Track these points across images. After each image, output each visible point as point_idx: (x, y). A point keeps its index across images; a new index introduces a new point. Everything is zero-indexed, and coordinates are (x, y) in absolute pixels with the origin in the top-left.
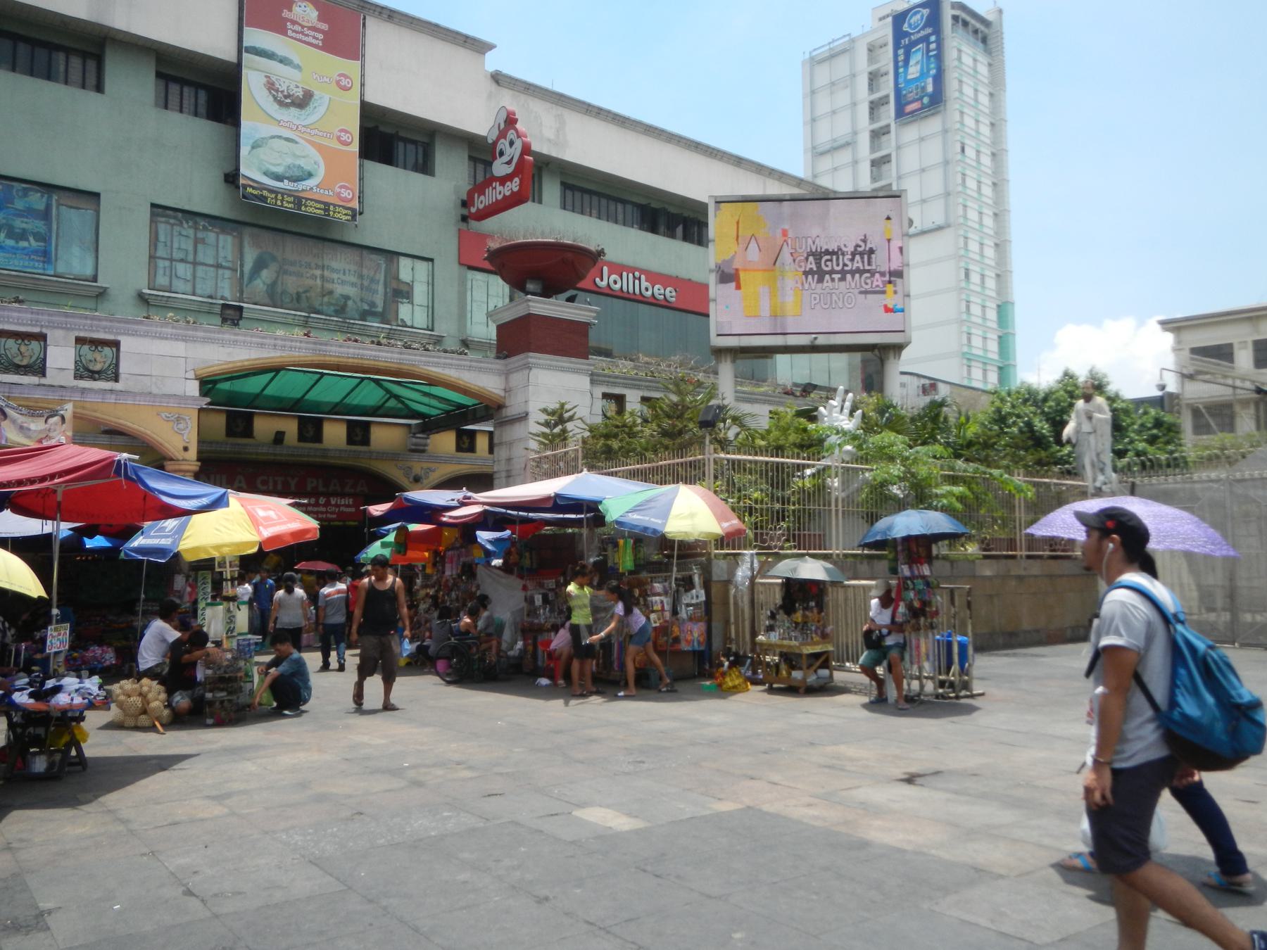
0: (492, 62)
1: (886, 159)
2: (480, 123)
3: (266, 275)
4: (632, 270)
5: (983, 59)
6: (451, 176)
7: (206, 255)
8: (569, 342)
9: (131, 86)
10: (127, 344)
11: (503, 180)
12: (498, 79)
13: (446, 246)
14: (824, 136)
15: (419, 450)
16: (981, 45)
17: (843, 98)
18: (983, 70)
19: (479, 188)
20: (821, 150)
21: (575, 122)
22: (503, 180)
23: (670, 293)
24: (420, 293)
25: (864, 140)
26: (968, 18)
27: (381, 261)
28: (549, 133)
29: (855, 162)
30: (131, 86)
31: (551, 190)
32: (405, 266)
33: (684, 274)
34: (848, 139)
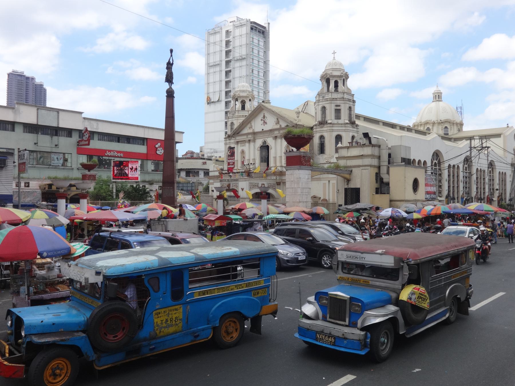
0: (83, 115)
1: (230, 71)
2: (81, 127)
3: (42, 159)
4: (113, 151)
5: (262, 40)
6: (75, 137)
7: (32, 157)
8: (93, 178)
9: (19, 129)
10: (31, 182)
11: (85, 141)
12: (84, 118)
13: (74, 151)
14: (212, 61)
15: (69, 190)
16: (262, 35)
17: (218, 48)
18: (262, 44)
19: (81, 141)
20: (210, 65)
21: (100, 124)
22: (85, 141)
23: (122, 155)
24: (69, 160)
25: (224, 63)
26: (257, 26)
27: (62, 154)
28: (95, 127)
29: (221, 71)
30: (19, 129)
31: (96, 137)
32: (66, 155)
33: (125, 151)
34: (219, 63)
